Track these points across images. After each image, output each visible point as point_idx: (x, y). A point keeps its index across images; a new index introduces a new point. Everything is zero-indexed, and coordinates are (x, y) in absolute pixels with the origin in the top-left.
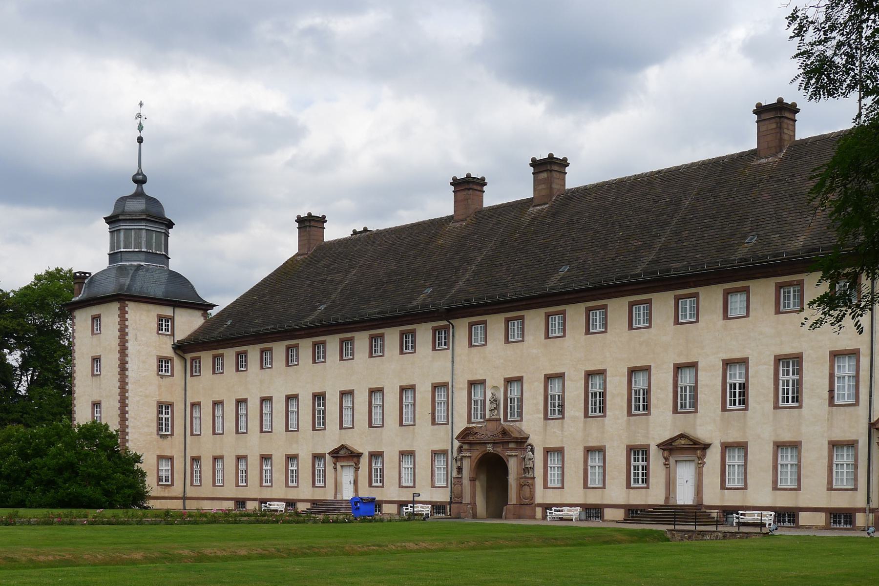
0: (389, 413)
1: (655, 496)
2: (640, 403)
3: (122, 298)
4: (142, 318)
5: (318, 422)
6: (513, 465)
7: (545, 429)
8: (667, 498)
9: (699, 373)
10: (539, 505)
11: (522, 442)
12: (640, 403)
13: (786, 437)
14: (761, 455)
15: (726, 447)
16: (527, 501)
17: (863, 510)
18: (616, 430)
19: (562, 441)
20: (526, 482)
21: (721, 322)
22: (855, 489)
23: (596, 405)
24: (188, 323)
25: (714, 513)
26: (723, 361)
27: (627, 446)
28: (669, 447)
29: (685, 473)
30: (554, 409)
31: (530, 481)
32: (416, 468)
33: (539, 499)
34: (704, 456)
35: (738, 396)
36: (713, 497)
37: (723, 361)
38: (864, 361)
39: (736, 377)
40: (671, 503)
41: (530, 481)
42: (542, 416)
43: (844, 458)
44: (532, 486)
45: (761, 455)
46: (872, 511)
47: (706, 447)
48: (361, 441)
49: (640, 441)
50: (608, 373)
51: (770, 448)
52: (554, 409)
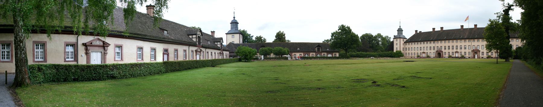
0: (429, 48)
1: (454, 56)
2: (453, 49)
3: (400, 38)
4: (402, 40)
5: (421, 50)
11: (442, 52)
12: (453, 49)
18: (451, 51)
23: (449, 49)
24: (405, 40)
29: (457, 54)
30: (445, 49)
32: (432, 53)
35: (461, 48)
48: (426, 51)
52: (445, 49)
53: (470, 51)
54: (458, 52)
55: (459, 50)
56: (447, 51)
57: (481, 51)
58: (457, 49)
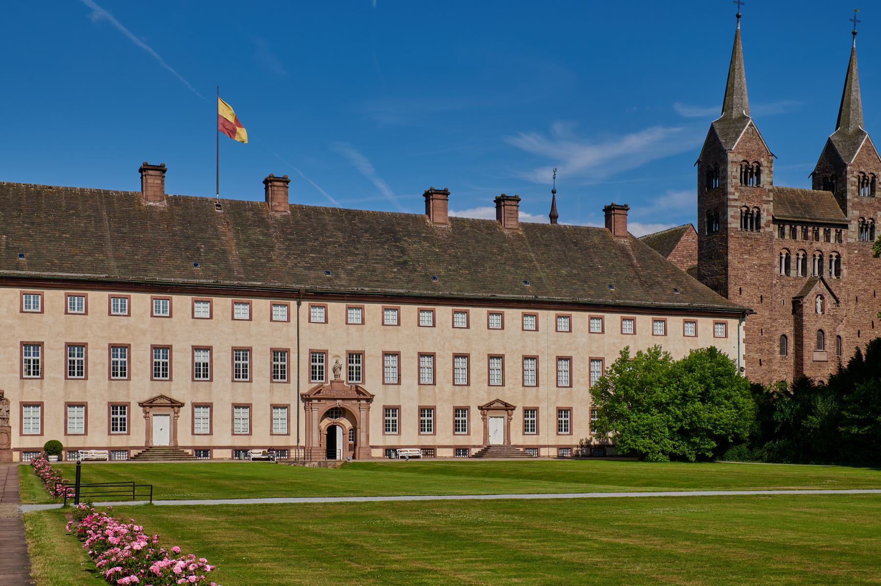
1: (136, 438)
2: (119, 371)
7: (22, 386)
8: (147, 442)
9: (174, 353)
10: (16, 450)
12: (119, 371)
13: (241, 400)
14: (223, 412)
15: (196, 405)
16: (5, 447)
17: (297, 447)
19: (41, 397)
21: (191, 320)
22: (288, 434)
25: (190, 452)
26: (192, 346)
27: (109, 403)
28: (148, 405)
31: (7, 429)
33: (13, 445)
34: (179, 411)
35: (202, 372)
36: (185, 440)
37: (192, 346)
38: (293, 357)
39: (202, 357)
40: (150, 445)
41: (7, 429)
42: (18, 375)
43: (280, 414)
44: (8, 434)
45: (223, 412)
46: (302, 447)
47: (182, 405)
49: (121, 399)
50: (89, 346)
51: (230, 407)
53: (287, 393)
54: (175, 405)
55: (181, 386)
56: (54, 386)
57: (382, 397)
58: (161, 372)
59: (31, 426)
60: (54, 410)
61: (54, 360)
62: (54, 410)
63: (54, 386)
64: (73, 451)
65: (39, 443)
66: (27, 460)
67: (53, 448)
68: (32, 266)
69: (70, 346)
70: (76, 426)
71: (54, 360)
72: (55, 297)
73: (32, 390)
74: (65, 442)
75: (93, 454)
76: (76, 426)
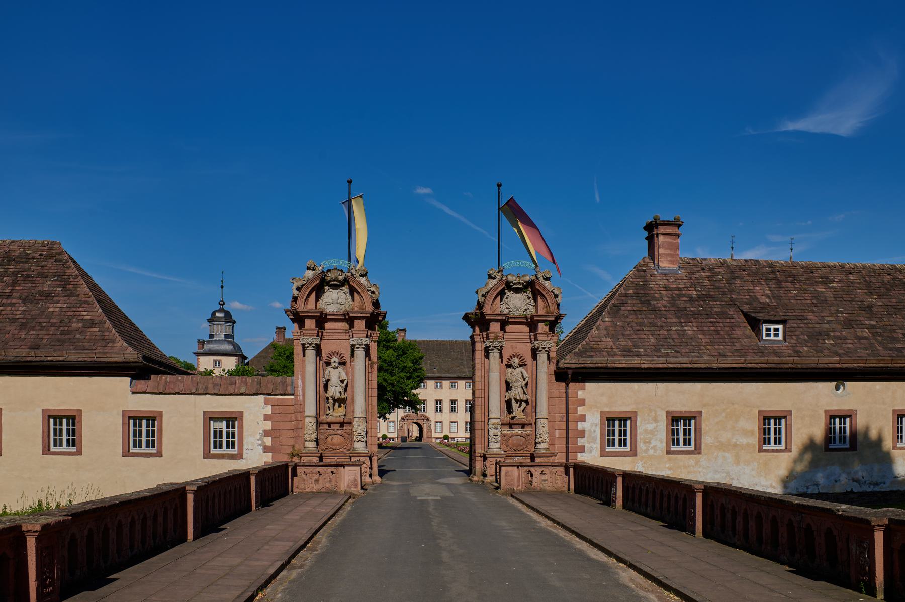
6: (425, 427)
11: (428, 419)
20: (430, 431)
30: (439, 409)
52: (439, 409)
56: (446, 415)
59: (439, 430)
60: (446, 424)
61: (446, 406)
62: (446, 424)
63: (446, 415)
64: (453, 438)
65: (442, 435)
66: (438, 441)
67: (446, 437)
68: (438, 372)
69: (452, 401)
70: (454, 430)
71: (446, 406)
72: (446, 383)
73: (439, 417)
74: (451, 435)
75: (459, 440)
76: (454, 430)
